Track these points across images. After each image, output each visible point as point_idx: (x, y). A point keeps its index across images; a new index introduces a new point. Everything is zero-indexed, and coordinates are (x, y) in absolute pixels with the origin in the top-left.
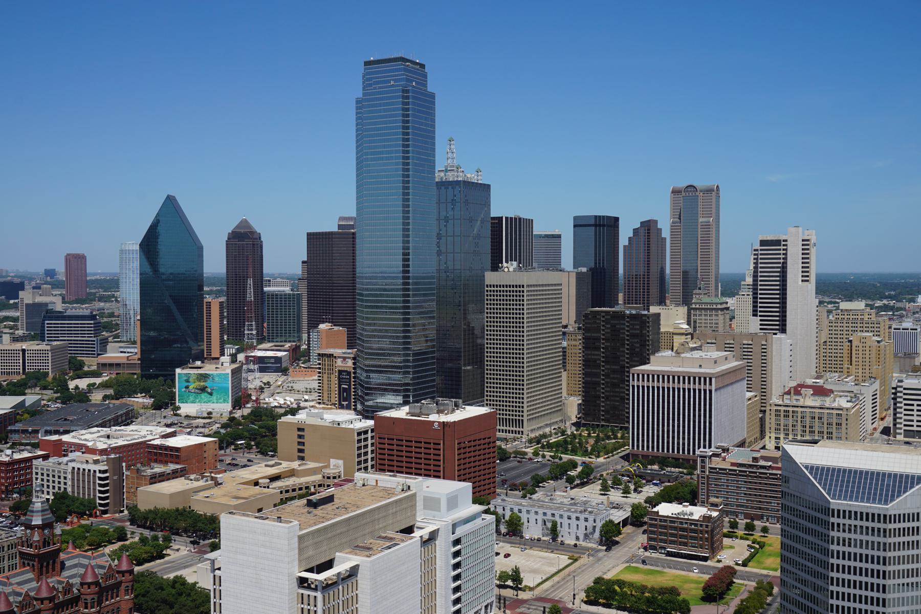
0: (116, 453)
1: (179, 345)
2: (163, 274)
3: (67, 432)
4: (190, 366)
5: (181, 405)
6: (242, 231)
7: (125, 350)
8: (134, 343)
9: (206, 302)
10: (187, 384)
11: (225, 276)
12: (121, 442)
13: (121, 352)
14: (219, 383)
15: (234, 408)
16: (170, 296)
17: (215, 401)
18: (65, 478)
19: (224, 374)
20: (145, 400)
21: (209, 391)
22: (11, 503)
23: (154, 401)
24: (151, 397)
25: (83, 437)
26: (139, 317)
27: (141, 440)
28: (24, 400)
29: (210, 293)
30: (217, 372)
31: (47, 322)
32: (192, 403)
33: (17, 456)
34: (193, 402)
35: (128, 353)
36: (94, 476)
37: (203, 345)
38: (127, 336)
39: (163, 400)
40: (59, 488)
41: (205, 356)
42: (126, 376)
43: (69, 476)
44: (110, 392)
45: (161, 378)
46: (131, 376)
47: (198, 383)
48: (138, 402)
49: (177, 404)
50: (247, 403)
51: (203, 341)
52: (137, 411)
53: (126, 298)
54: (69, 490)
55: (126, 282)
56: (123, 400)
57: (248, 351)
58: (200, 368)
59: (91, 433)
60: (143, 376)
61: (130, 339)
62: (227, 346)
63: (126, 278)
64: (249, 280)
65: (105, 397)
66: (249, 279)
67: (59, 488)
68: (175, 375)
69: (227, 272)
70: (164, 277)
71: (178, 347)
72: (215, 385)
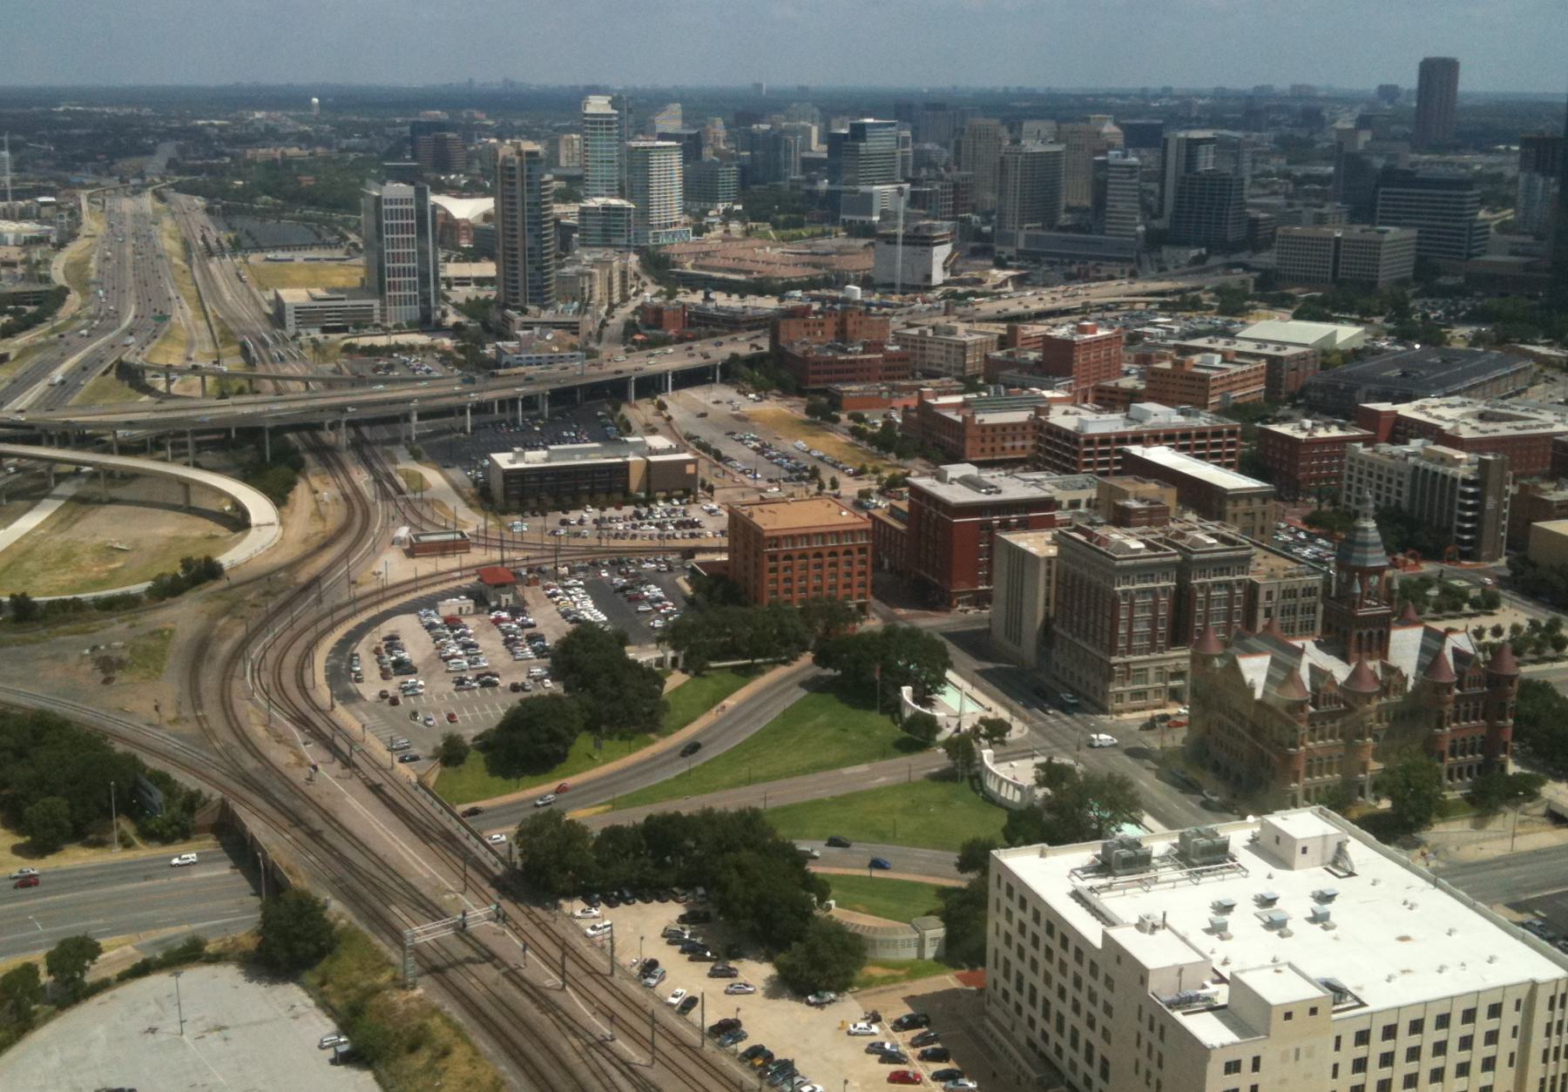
0: (1495, 451)
3: (1407, 398)
12: (1504, 430)
18: (1400, 484)
22: (1307, 512)
25: (1435, 412)
27: (1541, 431)
28: (1334, 334)
31: (1382, 189)
33: (1321, 433)
36: (1453, 489)
40: (1388, 499)
43: (1407, 482)
54: (1405, 505)
59: (1450, 406)
65: (1477, 339)
67: (1388, 499)
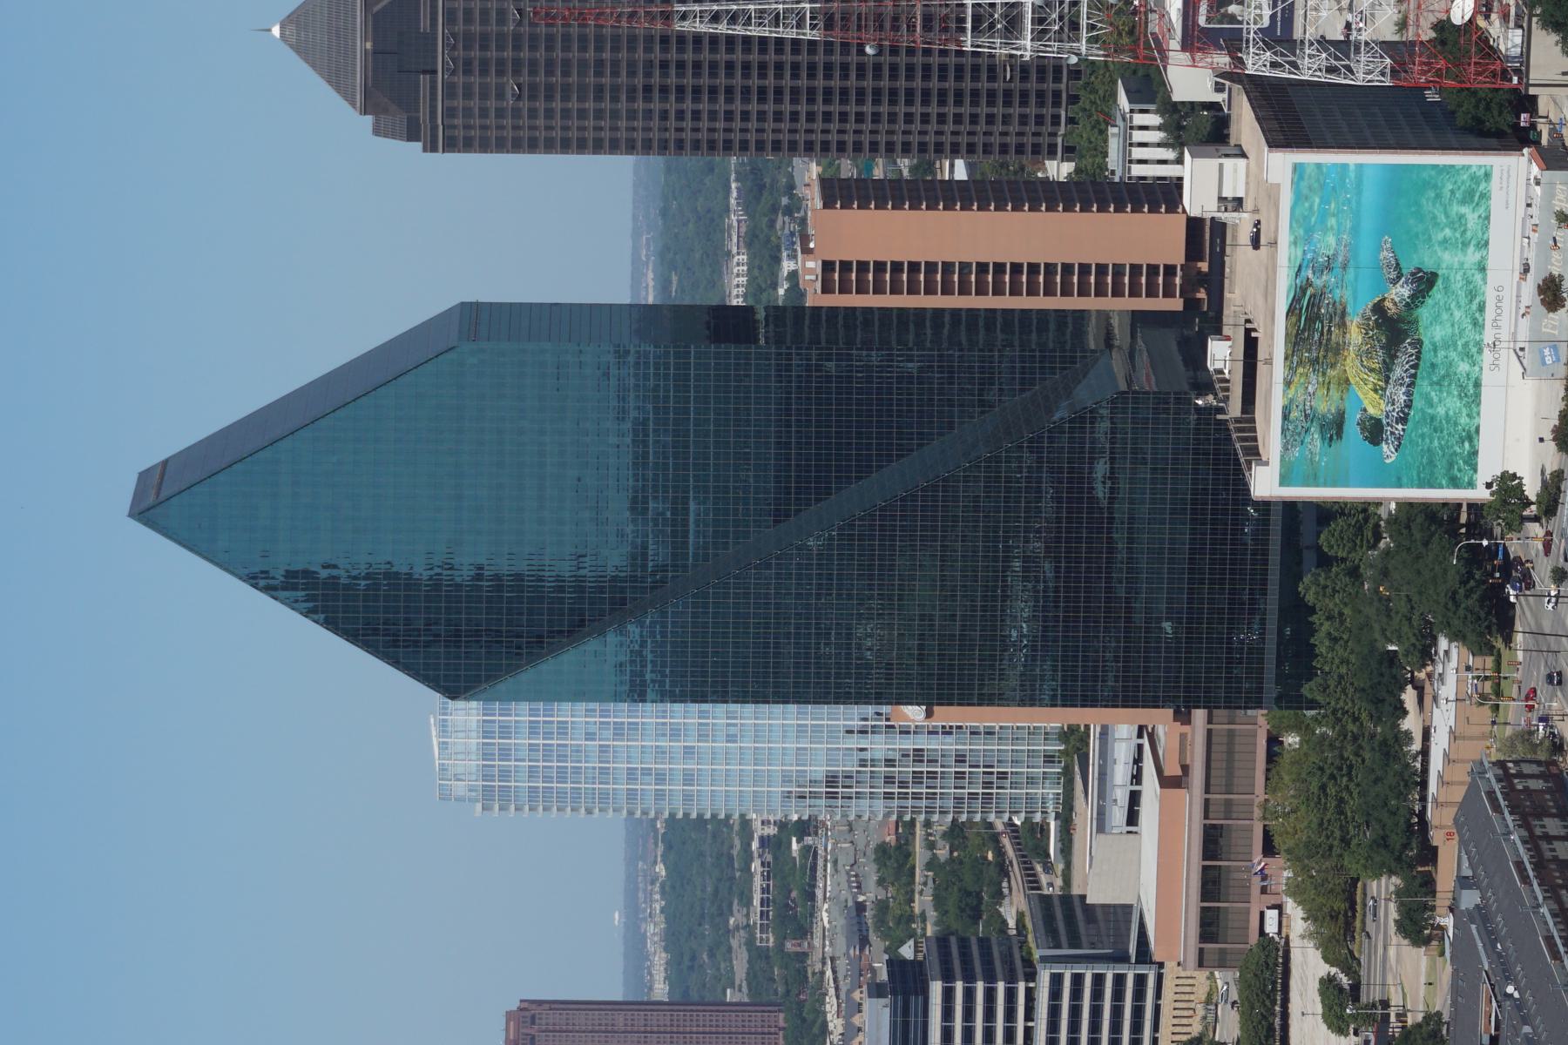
1: (1101, 468)
2: (639, 555)
4: (1235, 409)
5: (1488, 469)
6: (362, 45)
7: (1121, 795)
8: (1075, 740)
9: (827, 289)
10: (1352, 430)
11: (656, 161)
13: (1132, 818)
14: (1355, 230)
15: (1520, 139)
16: (780, 516)
17: (1472, 256)
19: (1299, 197)
20: (1448, 690)
21: (1401, 291)
23: (1455, 636)
24: (1426, 654)
26: (914, 713)
29: (765, 255)
30: (1284, 238)
32: (1476, 399)
34: (1472, 394)
35: (1137, 778)
37: (1104, 316)
38: (1031, 781)
39: (1453, 579)
41: (1176, 304)
42: (1287, 797)
44: (1382, 890)
45: (1308, 589)
46: (1285, 760)
47: (1351, 364)
48: (1454, 735)
49: (1481, 494)
50: (1487, 49)
51: (1081, 315)
52: (1511, 743)
53: (786, 779)
55: (688, 778)
56: (1441, 820)
57: (1154, 26)
58: (1251, 345)
60: (1291, 700)
61: (1049, 759)
62: (1113, 160)
63: (660, 778)
64: (686, 26)
65: (1416, 927)
66: (679, 26)
68: (1290, 507)
69: (631, 148)
70: (658, 553)
71: (1112, 476)
72: (1365, 255)
